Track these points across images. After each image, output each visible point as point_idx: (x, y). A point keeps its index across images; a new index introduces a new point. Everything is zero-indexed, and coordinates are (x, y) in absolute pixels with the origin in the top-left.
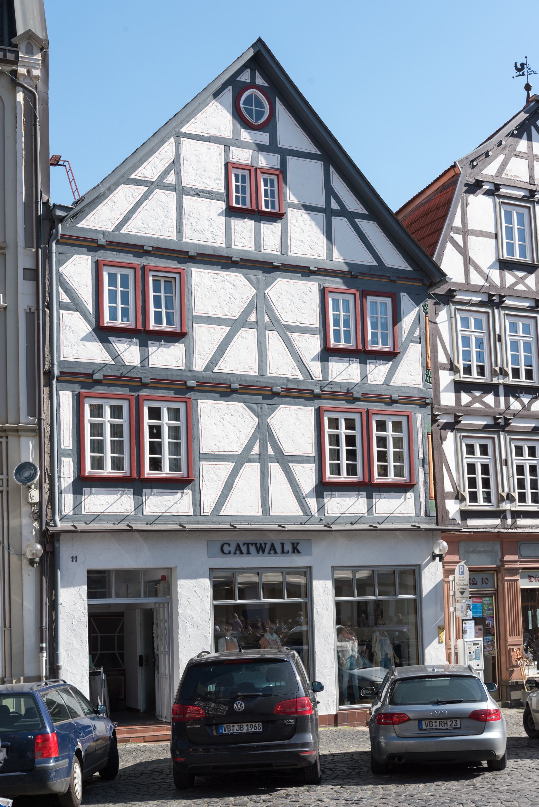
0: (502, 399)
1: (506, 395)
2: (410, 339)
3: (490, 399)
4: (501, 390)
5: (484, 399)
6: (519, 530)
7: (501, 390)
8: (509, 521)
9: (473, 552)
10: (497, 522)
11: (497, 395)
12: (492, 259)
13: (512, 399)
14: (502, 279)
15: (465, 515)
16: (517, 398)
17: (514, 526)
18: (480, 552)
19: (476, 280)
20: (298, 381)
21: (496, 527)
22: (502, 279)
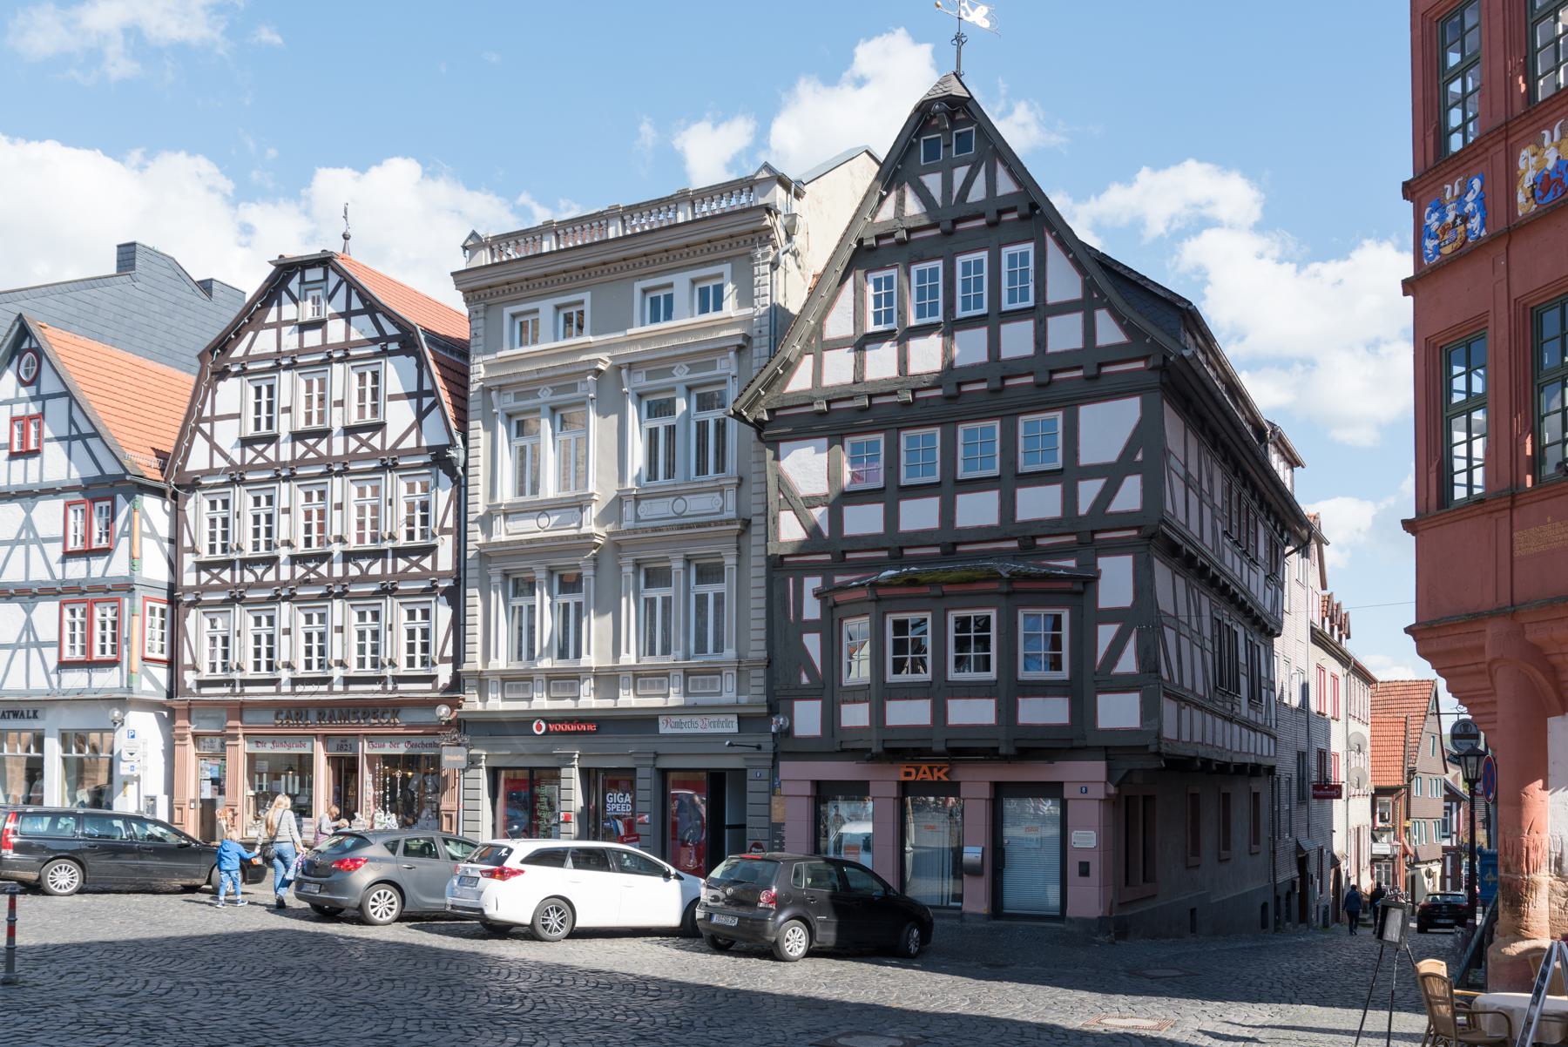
0: (238, 572)
1: (242, 569)
2: (123, 534)
3: (226, 575)
4: (238, 565)
5: (221, 576)
6: (246, 698)
7: (238, 565)
8: (238, 689)
9: (203, 718)
10: (227, 690)
11: (233, 570)
12: (234, 439)
13: (246, 572)
14: (243, 455)
15: (201, 684)
16: (251, 571)
17: (242, 693)
18: (208, 718)
19: (220, 463)
20: (48, 582)
21: (226, 695)
22: (243, 455)
